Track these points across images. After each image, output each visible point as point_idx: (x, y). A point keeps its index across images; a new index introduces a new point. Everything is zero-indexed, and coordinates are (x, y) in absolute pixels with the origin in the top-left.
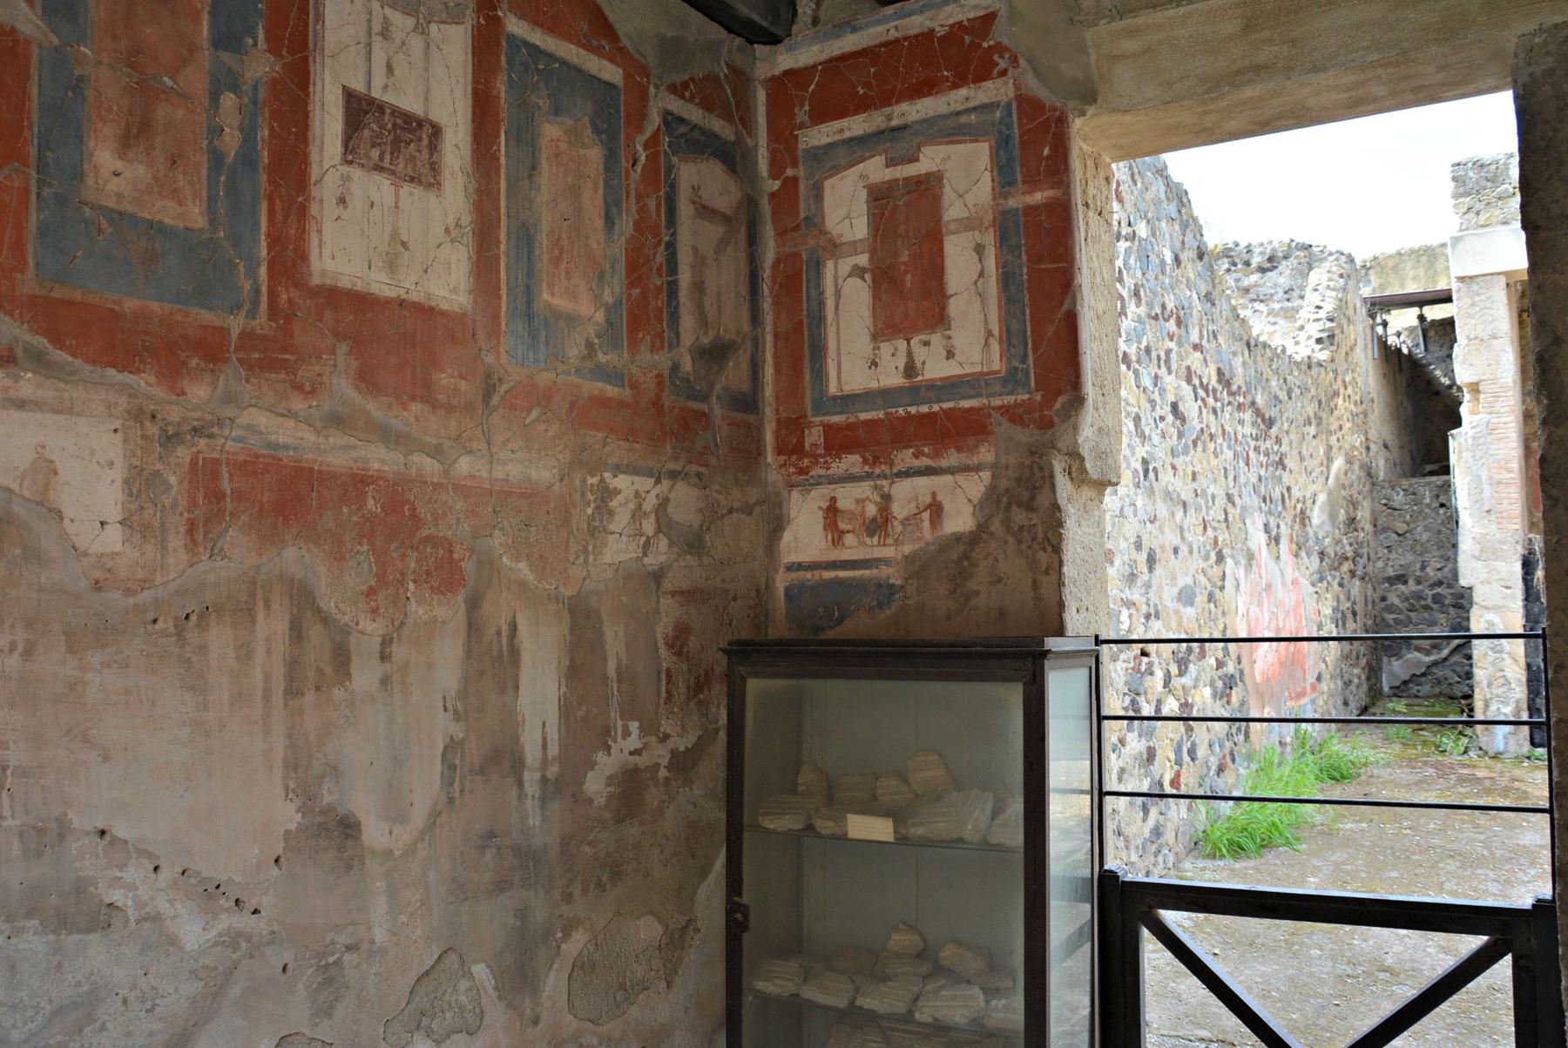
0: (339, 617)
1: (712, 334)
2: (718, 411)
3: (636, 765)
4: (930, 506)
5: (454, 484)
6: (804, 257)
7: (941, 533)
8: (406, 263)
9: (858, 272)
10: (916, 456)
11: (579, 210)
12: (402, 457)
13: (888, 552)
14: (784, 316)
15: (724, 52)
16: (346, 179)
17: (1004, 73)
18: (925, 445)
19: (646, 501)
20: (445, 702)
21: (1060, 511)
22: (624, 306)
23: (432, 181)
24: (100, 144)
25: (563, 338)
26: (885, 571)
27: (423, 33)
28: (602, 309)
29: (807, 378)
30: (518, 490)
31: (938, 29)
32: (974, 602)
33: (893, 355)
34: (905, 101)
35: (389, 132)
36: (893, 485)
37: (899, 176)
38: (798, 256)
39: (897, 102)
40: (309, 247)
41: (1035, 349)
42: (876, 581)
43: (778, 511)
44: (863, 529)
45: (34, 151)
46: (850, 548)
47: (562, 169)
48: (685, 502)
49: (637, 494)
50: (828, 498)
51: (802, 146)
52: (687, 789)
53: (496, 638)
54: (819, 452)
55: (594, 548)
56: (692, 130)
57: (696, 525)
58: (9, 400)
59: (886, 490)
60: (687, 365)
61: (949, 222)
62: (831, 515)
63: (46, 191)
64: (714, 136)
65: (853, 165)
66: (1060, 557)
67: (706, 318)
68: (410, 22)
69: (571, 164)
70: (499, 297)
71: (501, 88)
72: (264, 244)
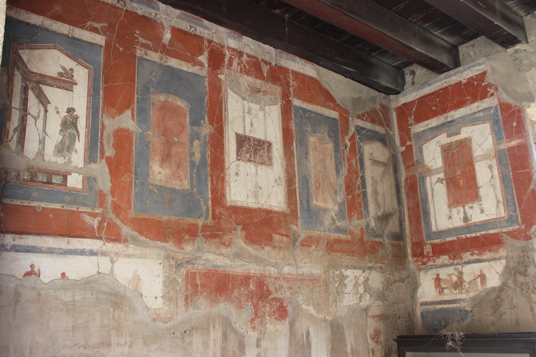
0: (240, 331)
1: (382, 211)
2: (387, 241)
4: (480, 276)
5: (283, 277)
6: (417, 176)
7: (486, 287)
9: (440, 180)
10: (472, 255)
11: (325, 168)
12: (262, 267)
13: (463, 296)
14: (411, 200)
15: (378, 100)
16: (238, 166)
17: (492, 95)
18: (475, 250)
22: (346, 203)
23: (269, 163)
25: (322, 218)
26: (463, 305)
27: (263, 110)
29: (423, 225)
31: (463, 81)
32: (504, 317)
33: (458, 213)
34: (452, 111)
35: (253, 147)
36: (463, 268)
37: (453, 141)
38: (414, 176)
39: (449, 111)
40: (226, 192)
41: (519, 206)
43: (415, 281)
44: (452, 287)
45: (133, 168)
46: (447, 295)
47: (318, 153)
49: (356, 277)
50: (436, 274)
51: (412, 132)
53: (301, 337)
55: (339, 300)
57: (381, 289)
59: (460, 270)
60: (373, 224)
61: (476, 157)
63: (138, 181)
64: (376, 133)
68: (258, 107)
69: (321, 150)
70: (297, 204)
71: (293, 126)
72: (210, 192)
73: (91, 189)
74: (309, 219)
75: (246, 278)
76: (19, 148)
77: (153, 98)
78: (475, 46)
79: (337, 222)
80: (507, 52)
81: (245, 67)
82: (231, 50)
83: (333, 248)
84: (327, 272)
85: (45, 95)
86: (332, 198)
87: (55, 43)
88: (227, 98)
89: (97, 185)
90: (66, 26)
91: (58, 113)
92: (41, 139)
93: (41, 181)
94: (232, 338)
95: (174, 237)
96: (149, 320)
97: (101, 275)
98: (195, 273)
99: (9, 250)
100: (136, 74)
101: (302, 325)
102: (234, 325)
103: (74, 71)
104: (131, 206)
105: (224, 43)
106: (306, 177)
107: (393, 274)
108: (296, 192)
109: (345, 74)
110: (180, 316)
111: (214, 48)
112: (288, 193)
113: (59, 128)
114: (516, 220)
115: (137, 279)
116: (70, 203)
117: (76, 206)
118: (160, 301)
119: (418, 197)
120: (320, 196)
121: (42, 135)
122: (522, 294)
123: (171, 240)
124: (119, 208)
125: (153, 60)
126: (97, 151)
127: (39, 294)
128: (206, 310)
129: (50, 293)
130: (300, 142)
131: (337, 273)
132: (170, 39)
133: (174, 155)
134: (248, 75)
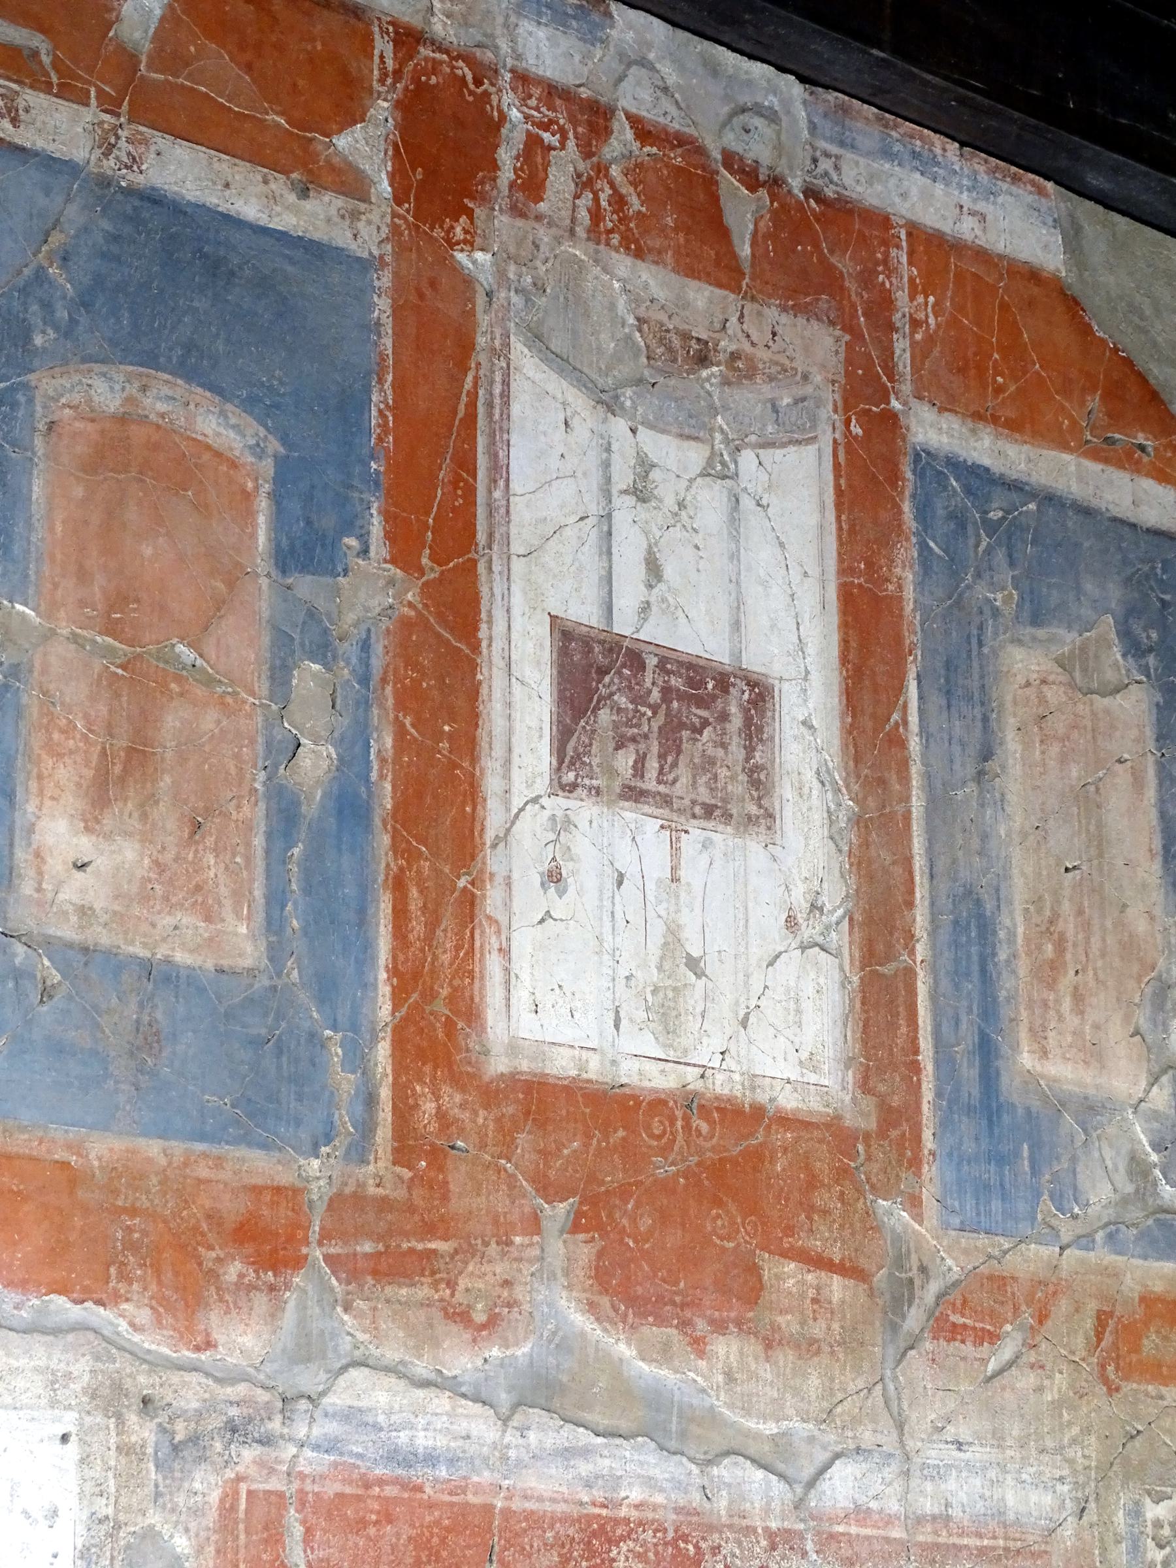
5: (818, 1533)
8: (699, 1009)
11: (1099, 842)
16: (563, 825)
23: (753, 809)
24: (48, 803)
25: (1074, 1160)
35: (655, 709)
40: (482, 987)
47: (1055, 749)
68: (695, 456)
69: (1075, 735)
70: (916, 1068)
72: (384, 990)
74: (993, 1168)
75: (594, 1534)
77: (51, 393)
81: (619, 201)
82: (536, 92)
83: (1136, 1349)
88: (506, 396)
95: (158, 1273)
105: (496, 49)
106: (978, 902)
108: (912, 992)
111: (433, 80)
112: (863, 1004)
120: (1061, 1018)
123: (135, 1286)
130: (947, 681)
132: (162, 19)
133: (169, 754)
134: (639, 254)
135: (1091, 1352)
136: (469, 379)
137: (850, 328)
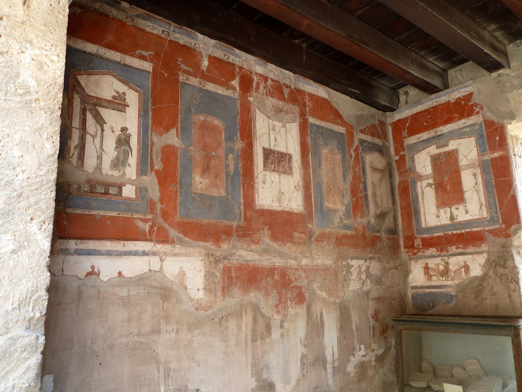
0: (267, 315)
1: (380, 210)
2: (384, 235)
3: (364, 360)
4: (464, 266)
5: (301, 268)
6: (409, 181)
10: (457, 248)
11: (335, 175)
12: (285, 260)
13: (449, 283)
15: (377, 116)
16: (265, 175)
17: (478, 113)
18: (460, 245)
19: (362, 268)
20: (301, 341)
21: (517, 268)
22: (351, 204)
23: (290, 172)
24: (196, 174)
26: (449, 290)
28: (344, 206)
29: (414, 222)
30: (321, 268)
32: (485, 302)
33: (445, 213)
37: (442, 152)
38: (406, 181)
39: (439, 127)
41: (500, 209)
42: (445, 293)
43: (407, 268)
44: (439, 274)
45: (179, 179)
46: (435, 281)
47: (329, 163)
48: (375, 267)
49: (359, 266)
51: (405, 144)
52: (382, 369)
54: (420, 247)
55: (346, 285)
56: (368, 144)
57: (379, 275)
58: (173, 254)
59: (447, 260)
60: (373, 221)
61: (462, 166)
62: (427, 269)
63: (182, 190)
64: (375, 144)
65: (424, 149)
66: (519, 285)
67: (378, 205)
68: (281, 124)
72: (242, 198)
73: (143, 198)
75: (272, 270)
76: (80, 163)
78: (463, 70)
79: (344, 221)
80: (491, 76)
81: (269, 90)
84: (336, 263)
85: (101, 116)
86: (340, 200)
87: (109, 70)
88: (255, 117)
89: (148, 194)
90: (118, 53)
91: (113, 131)
92: (99, 155)
93: (99, 192)
94: (261, 322)
96: (193, 309)
97: (152, 272)
98: (230, 267)
99: (72, 253)
100: (180, 97)
101: (317, 308)
102: (262, 310)
103: (126, 94)
104: (176, 211)
105: (252, 70)
107: (389, 263)
109: (351, 95)
110: (218, 304)
113: (115, 145)
114: (497, 220)
115: (182, 274)
116: (125, 211)
117: (130, 214)
118: (201, 293)
119: (410, 199)
120: (331, 199)
121: (100, 151)
122: (502, 283)
123: (210, 240)
124: (167, 214)
125: (193, 84)
126: (148, 165)
127: (99, 291)
128: (240, 298)
129: (108, 290)
131: (344, 263)
132: (208, 66)
133: (212, 167)
134: (272, 97)
135: (335, 242)
136: (250, 115)
137: (301, 107)
